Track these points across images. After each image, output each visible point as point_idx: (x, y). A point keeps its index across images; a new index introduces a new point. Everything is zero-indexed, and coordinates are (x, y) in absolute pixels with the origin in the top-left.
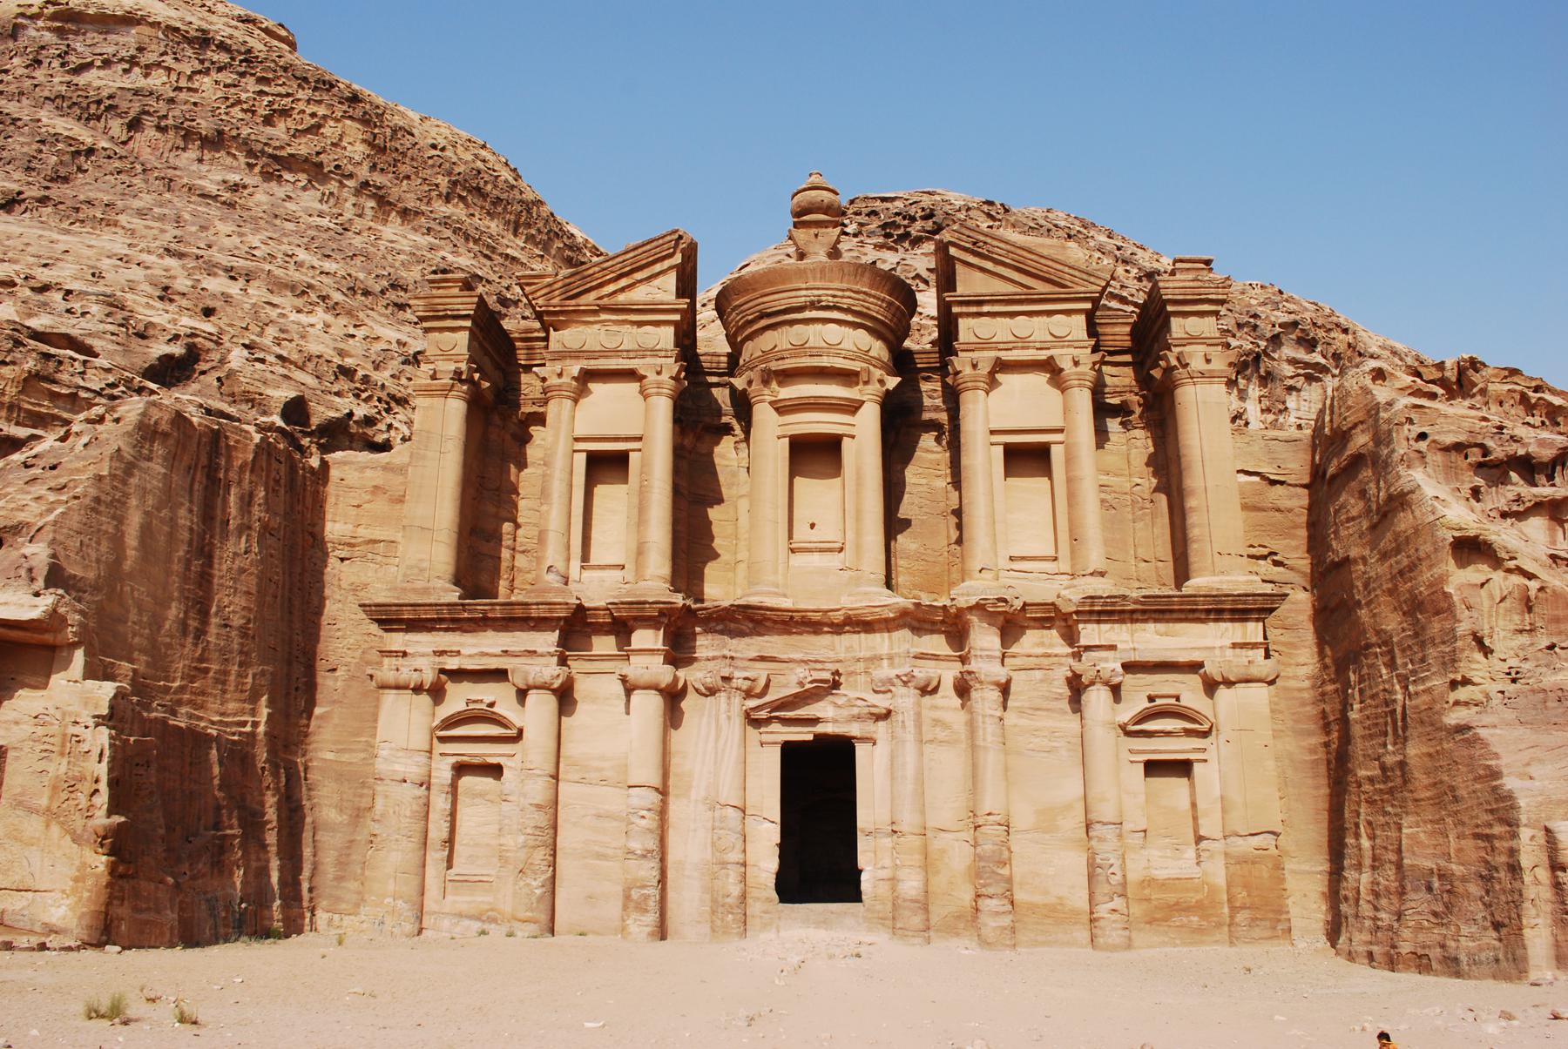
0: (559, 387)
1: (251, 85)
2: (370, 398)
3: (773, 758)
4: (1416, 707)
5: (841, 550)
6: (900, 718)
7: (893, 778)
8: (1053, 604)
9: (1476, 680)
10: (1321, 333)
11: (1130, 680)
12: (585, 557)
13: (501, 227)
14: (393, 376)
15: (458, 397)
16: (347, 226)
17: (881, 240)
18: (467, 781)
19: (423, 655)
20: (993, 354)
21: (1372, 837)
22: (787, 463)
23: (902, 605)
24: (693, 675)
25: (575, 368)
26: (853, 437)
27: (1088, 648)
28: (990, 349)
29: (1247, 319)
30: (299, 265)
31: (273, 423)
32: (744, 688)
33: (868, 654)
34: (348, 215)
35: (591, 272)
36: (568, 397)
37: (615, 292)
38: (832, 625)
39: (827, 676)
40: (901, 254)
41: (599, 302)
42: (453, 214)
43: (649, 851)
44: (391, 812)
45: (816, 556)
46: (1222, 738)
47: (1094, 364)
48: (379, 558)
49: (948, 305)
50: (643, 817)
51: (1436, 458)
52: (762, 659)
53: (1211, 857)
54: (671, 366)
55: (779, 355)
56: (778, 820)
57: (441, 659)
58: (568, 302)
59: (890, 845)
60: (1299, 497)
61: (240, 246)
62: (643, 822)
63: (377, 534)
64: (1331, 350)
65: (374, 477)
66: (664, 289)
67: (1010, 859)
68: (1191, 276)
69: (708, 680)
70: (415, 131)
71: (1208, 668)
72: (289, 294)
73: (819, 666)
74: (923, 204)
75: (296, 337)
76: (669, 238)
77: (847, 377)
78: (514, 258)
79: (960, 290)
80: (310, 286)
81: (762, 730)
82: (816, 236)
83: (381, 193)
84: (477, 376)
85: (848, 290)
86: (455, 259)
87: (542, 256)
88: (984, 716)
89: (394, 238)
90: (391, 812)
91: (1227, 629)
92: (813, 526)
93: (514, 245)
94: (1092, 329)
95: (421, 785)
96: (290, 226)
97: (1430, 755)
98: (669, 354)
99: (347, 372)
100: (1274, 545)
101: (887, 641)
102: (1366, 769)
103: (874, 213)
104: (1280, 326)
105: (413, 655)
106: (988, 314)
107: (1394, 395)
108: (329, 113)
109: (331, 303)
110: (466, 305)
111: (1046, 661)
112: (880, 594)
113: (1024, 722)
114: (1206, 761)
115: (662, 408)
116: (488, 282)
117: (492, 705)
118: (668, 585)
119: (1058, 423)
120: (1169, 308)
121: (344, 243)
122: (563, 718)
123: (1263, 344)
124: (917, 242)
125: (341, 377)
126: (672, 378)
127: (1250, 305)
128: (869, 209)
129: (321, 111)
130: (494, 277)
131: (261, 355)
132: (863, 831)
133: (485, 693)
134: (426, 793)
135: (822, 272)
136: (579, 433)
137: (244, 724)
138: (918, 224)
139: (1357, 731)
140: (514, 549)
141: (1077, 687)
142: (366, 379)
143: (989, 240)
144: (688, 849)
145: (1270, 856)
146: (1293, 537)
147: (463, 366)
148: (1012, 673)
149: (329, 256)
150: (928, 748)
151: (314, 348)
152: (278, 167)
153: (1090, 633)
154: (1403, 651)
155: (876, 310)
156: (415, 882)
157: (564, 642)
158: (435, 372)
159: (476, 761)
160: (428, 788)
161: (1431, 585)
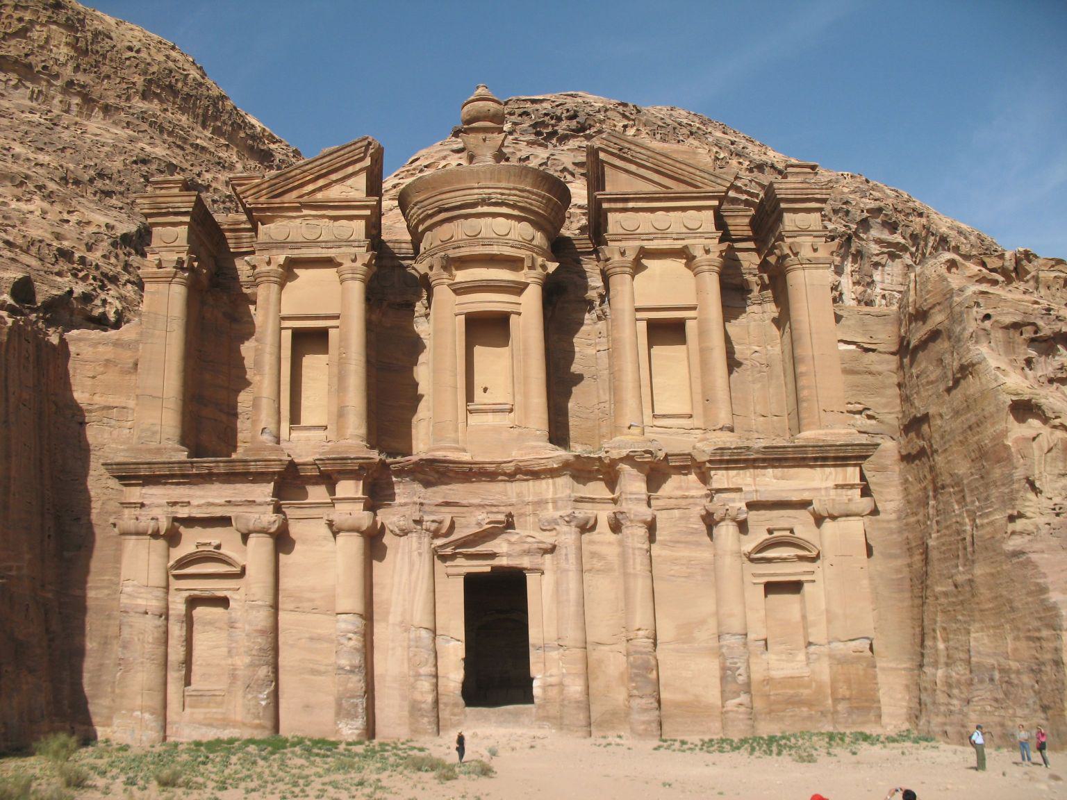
2: (86, 277)
3: (458, 587)
4: (981, 537)
5: (511, 411)
6: (564, 551)
8: (689, 454)
9: (1028, 514)
10: (901, 217)
11: (753, 517)
12: (295, 418)
14: (104, 256)
15: (181, 283)
16: (56, 121)
17: (533, 137)
18: (200, 612)
19: (159, 506)
21: (946, 640)
23: (564, 458)
24: (390, 517)
26: (519, 314)
27: (719, 491)
28: (635, 239)
30: (16, 157)
32: (432, 529)
33: (536, 499)
34: (56, 112)
35: (293, 173)
36: (275, 282)
37: (314, 191)
38: (505, 474)
39: (501, 517)
41: (300, 200)
42: (149, 109)
43: (356, 667)
44: (136, 639)
45: (490, 416)
46: (827, 563)
47: (721, 252)
48: (113, 422)
49: (600, 202)
51: (998, 335)
52: (447, 504)
53: (818, 659)
54: (364, 256)
55: (456, 244)
56: (463, 638)
57: (174, 509)
59: (557, 657)
60: (888, 362)
63: (111, 400)
64: (909, 231)
65: (106, 352)
66: (356, 188)
68: (800, 179)
69: (401, 523)
70: (113, 35)
71: (816, 505)
72: (10, 184)
73: (494, 509)
74: (567, 106)
75: (18, 223)
76: (359, 144)
77: (513, 263)
78: (203, 148)
79: (608, 189)
80: (27, 177)
81: (448, 563)
82: (484, 140)
84: (196, 264)
85: (515, 189)
86: (152, 150)
87: (227, 146)
88: (634, 549)
89: (99, 132)
90: (136, 639)
91: (830, 473)
93: (203, 137)
95: (161, 616)
97: (992, 575)
98: (362, 244)
99: (65, 254)
100: (870, 401)
101: (551, 486)
102: (942, 586)
103: (526, 114)
104: (868, 211)
105: (150, 506)
106: (633, 210)
107: (964, 282)
108: (34, 18)
109: (46, 192)
110: (186, 202)
111: (683, 503)
112: (545, 448)
113: (666, 553)
114: (814, 581)
115: (356, 290)
116: (183, 170)
117: (218, 547)
118: (364, 443)
119: (691, 302)
120: (783, 205)
121: (55, 137)
122: (282, 556)
123: (854, 226)
124: (563, 139)
126: (364, 265)
127: (843, 193)
128: (522, 110)
129: (28, 16)
130: (186, 165)
132: (534, 646)
133: (212, 536)
135: (492, 174)
136: (284, 313)
137: (10, 569)
138: (564, 124)
139: (934, 555)
141: (710, 521)
142: (82, 260)
143: (633, 147)
144: (388, 665)
147: (185, 256)
148: (656, 513)
149: (42, 149)
151: (34, 233)
153: (721, 478)
154: (972, 491)
155: (536, 205)
156: (159, 698)
157: (277, 493)
158: (160, 260)
160: (167, 619)
161: (993, 439)
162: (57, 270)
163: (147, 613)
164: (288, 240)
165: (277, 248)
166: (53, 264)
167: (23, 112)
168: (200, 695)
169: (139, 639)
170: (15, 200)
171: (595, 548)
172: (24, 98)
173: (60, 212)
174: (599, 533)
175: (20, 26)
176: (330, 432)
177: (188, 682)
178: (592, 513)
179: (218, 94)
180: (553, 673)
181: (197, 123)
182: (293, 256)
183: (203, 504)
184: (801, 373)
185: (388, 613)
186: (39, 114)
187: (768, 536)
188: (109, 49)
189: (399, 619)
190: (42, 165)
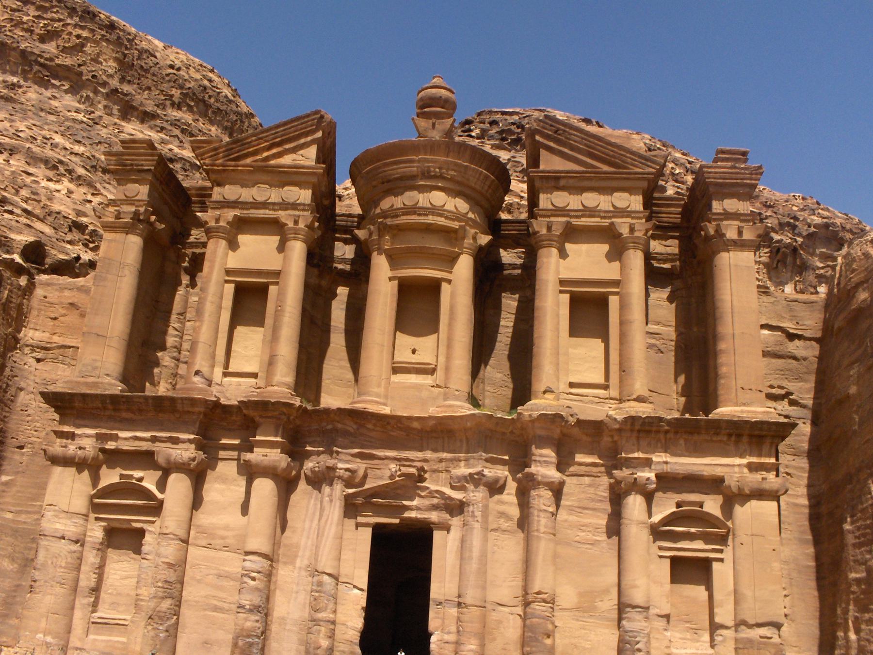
0: (218, 229)
1: (32, 11)
3: (366, 534)
6: (471, 508)
7: (462, 558)
8: (601, 422)
12: (227, 365)
13: (220, 131)
16: (97, 121)
19: (88, 436)
20: (564, 219)
21: (857, 631)
22: (395, 299)
25: (230, 214)
26: (449, 282)
28: (564, 216)
29: (788, 220)
30: (54, 146)
31: (13, 260)
32: (346, 476)
34: (98, 113)
36: (223, 238)
37: (267, 159)
39: (413, 470)
40: (512, 153)
41: (253, 163)
42: (182, 118)
44: (50, 562)
50: (254, 579)
54: (306, 218)
56: (365, 587)
58: (229, 163)
61: (10, 129)
62: (252, 583)
66: (308, 157)
67: (553, 631)
69: (317, 469)
70: (158, 54)
72: (43, 166)
75: (43, 198)
79: (542, 167)
80: (61, 162)
83: (127, 98)
84: (153, 218)
89: (134, 132)
90: (50, 562)
92: (414, 352)
94: (648, 203)
95: (77, 542)
96: (52, 118)
99: (80, 227)
100: (791, 386)
102: (856, 572)
103: (493, 123)
105: (80, 436)
108: (90, 35)
112: (462, 407)
113: (573, 518)
114: (721, 560)
115: (298, 249)
117: (141, 479)
119: (617, 276)
123: (800, 240)
125: (73, 229)
128: (491, 119)
129: (85, 34)
131: (10, 208)
132: (434, 601)
134: (80, 549)
140: (178, 360)
145: (775, 645)
146: (805, 381)
147: (142, 210)
149: (79, 142)
150: (492, 535)
151: (56, 207)
152: (49, 74)
159: (125, 526)
160: (82, 545)
162: (69, 239)
163: (64, 538)
164: (240, 200)
165: (228, 207)
166: (66, 234)
167: (69, 111)
168: (104, 624)
169: (52, 563)
170: (45, 179)
171: (502, 508)
172: (73, 101)
173: (85, 193)
174: (508, 494)
175: (78, 41)
176: (260, 382)
177: (95, 606)
178: (502, 474)
179: (245, 110)
180: (451, 631)
181: (225, 134)
182: (242, 215)
183: (131, 438)
184: (720, 350)
185: (296, 556)
186: (83, 114)
187: (674, 509)
188: (152, 65)
189: (306, 562)
190: (76, 154)
